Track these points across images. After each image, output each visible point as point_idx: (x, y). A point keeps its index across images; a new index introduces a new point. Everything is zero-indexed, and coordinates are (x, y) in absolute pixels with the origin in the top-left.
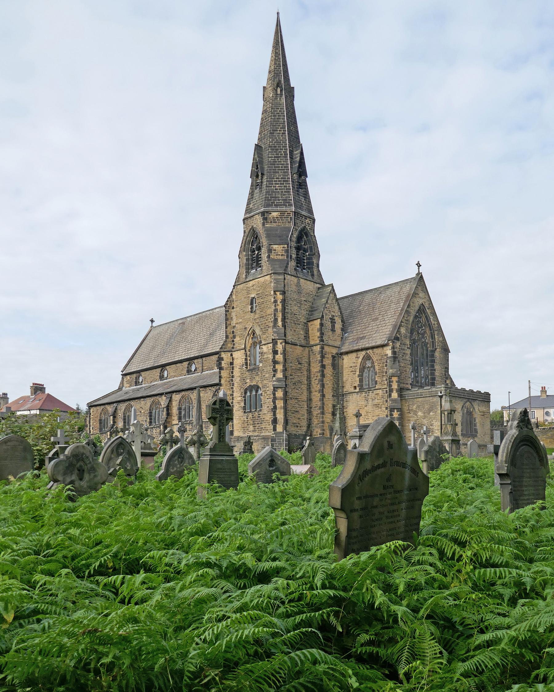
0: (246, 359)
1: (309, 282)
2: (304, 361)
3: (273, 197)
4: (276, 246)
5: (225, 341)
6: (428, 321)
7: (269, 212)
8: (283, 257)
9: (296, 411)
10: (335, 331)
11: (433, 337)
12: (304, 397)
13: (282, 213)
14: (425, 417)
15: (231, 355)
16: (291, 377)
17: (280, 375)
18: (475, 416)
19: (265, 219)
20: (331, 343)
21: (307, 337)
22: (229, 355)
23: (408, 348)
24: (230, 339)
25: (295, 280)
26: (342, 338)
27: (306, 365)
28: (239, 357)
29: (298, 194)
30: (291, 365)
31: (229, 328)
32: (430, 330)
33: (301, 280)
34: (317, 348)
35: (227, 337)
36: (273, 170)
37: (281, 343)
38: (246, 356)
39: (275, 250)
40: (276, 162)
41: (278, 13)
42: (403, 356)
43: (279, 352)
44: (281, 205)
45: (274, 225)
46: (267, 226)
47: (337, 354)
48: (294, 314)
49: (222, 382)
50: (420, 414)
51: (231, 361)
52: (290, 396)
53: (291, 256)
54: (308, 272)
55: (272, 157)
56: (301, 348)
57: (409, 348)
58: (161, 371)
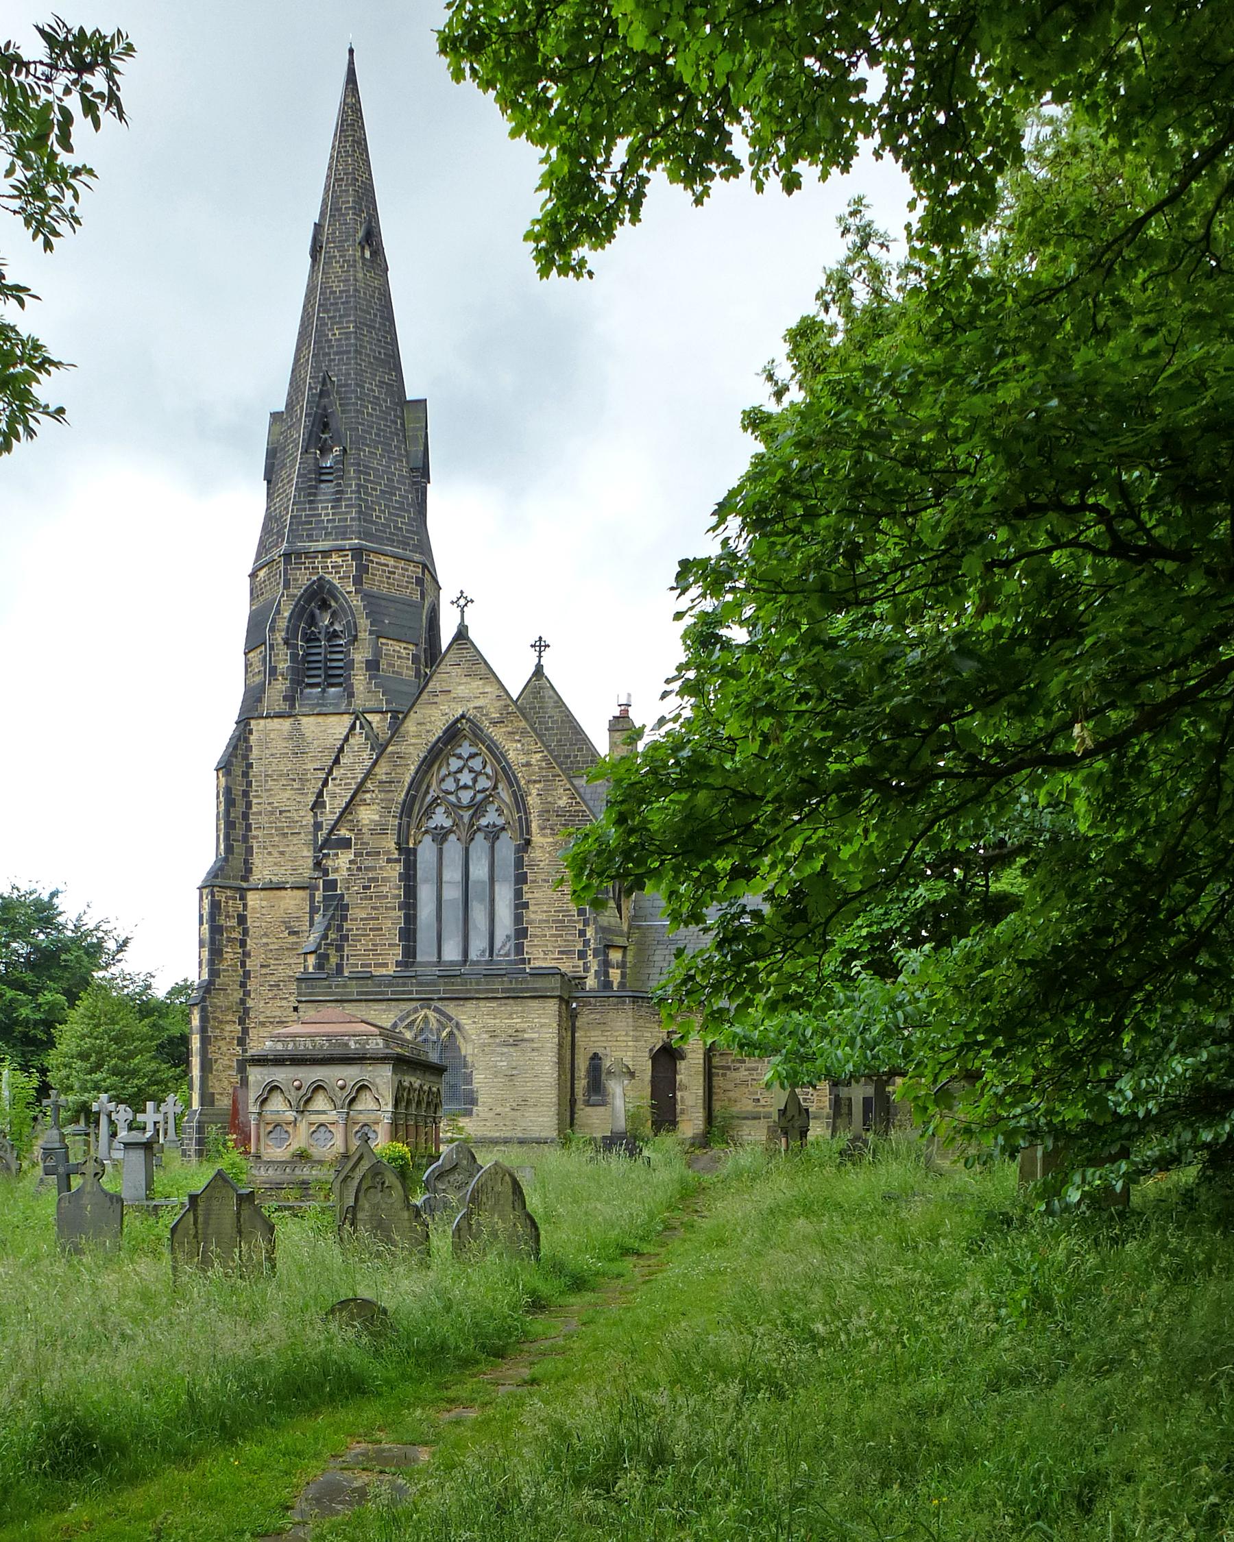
6: (499, 762)
16: (264, 971)
18: (466, 1049)
23: (389, 861)
25: (286, 724)
30: (265, 940)
32: (511, 786)
33: (304, 720)
48: (281, 812)
53: (273, 671)
57: (398, 861)
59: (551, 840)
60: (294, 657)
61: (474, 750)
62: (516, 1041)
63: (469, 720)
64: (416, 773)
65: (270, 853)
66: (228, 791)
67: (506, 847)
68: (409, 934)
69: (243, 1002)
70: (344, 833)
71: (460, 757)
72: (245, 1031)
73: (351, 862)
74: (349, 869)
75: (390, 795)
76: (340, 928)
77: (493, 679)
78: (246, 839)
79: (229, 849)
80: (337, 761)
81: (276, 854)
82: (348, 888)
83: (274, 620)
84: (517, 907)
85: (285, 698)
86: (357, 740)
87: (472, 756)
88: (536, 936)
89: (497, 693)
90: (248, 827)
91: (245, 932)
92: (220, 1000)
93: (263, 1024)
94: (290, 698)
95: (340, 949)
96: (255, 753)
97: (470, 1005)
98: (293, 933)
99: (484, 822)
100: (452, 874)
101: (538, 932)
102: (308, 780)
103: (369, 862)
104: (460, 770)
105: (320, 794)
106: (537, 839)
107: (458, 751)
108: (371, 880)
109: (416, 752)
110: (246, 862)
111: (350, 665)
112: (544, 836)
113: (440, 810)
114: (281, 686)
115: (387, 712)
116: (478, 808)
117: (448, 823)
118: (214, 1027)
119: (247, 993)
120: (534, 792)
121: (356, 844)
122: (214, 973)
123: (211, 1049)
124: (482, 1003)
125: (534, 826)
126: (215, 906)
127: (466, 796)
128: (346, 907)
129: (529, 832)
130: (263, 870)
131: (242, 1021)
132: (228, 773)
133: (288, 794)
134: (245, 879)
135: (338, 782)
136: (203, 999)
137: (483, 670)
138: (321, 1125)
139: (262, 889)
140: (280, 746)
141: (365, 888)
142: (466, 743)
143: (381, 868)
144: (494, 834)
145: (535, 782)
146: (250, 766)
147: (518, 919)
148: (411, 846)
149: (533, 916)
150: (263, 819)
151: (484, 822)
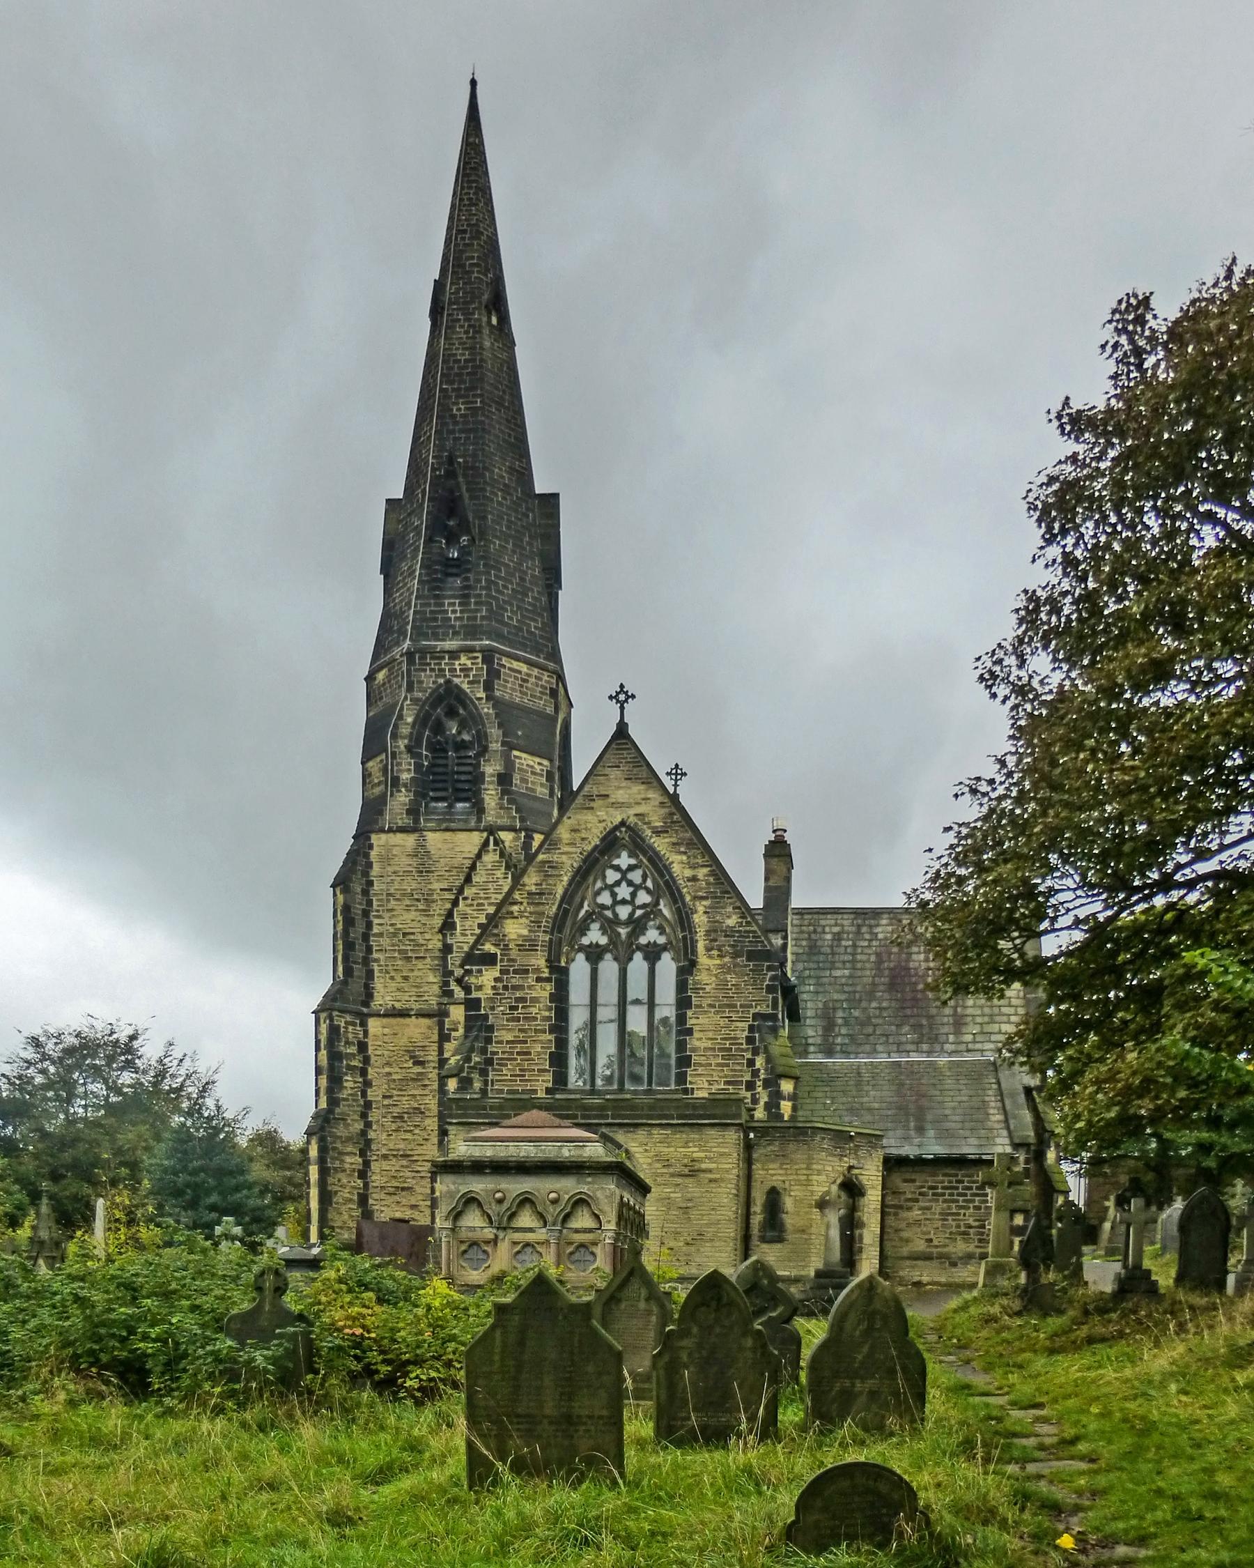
6: (662, 876)
9: (403, 1189)
16: (386, 1102)
23: (539, 980)
25: (410, 840)
30: (387, 1070)
32: (675, 902)
33: (430, 836)
48: (405, 934)
53: (396, 782)
57: (548, 980)
59: (718, 962)
60: (418, 767)
61: (633, 861)
62: (693, 1172)
63: (629, 828)
64: (570, 884)
65: (392, 978)
66: (347, 909)
67: (667, 966)
68: (559, 1060)
69: (363, 1133)
70: (489, 947)
71: (617, 868)
72: (367, 1164)
73: (496, 980)
74: (494, 988)
75: (541, 908)
76: (484, 1051)
77: (655, 784)
78: (366, 961)
79: (348, 972)
80: (468, 880)
81: (399, 979)
82: (493, 1008)
83: (396, 726)
84: (679, 1033)
85: (409, 812)
86: (490, 858)
87: (631, 868)
88: (700, 1065)
89: (661, 799)
90: (369, 950)
91: (366, 1060)
92: (340, 1131)
93: (385, 1157)
94: (413, 811)
95: (484, 1073)
96: (376, 870)
97: (641, 1134)
98: (417, 1063)
99: (643, 940)
100: (608, 994)
101: (702, 1060)
102: (433, 901)
103: (516, 980)
104: (618, 883)
105: (450, 914)
106: (703, 959)
107: (616, 862)
108: (518, 1000)
109: (570, 862)
110: (367, 986)
111: (479, 778)
112: (710, 957)
113: (595, 926)
114: (403, 798)
115: (520, 830)
116: (638, 926)
117: (603, 941)
118: (333, 1159)
119: (368, 1125)
120: (701, 909)
121: (502, 960)
122: (333, 1102)
123: (330, 1180)
124: (655, 1131)
125: (701, 946)
126: (334, 1031)
127: (624, 912)
128: (491, 1029)
129: (694, 952)
130: (385, 994)
131: (363, 1153)
132: (346, 891)
133: (413, 915)
134: (366, 1004)
135: (469, 902)
136: (322, 1129)
137: (644, 773)
138: (527, 1245)
139: (385, 1016)
140: (404, 863)
141: (512, 1008)
142: (624, 854)
143: (530, 987)
144: (653, 954)
145: (702, 898)
146: (370, 883)
147: (681, 1046)
148: (563, 964)
149: (697, 1044)
150: (385, 942)
151: (643, 940)
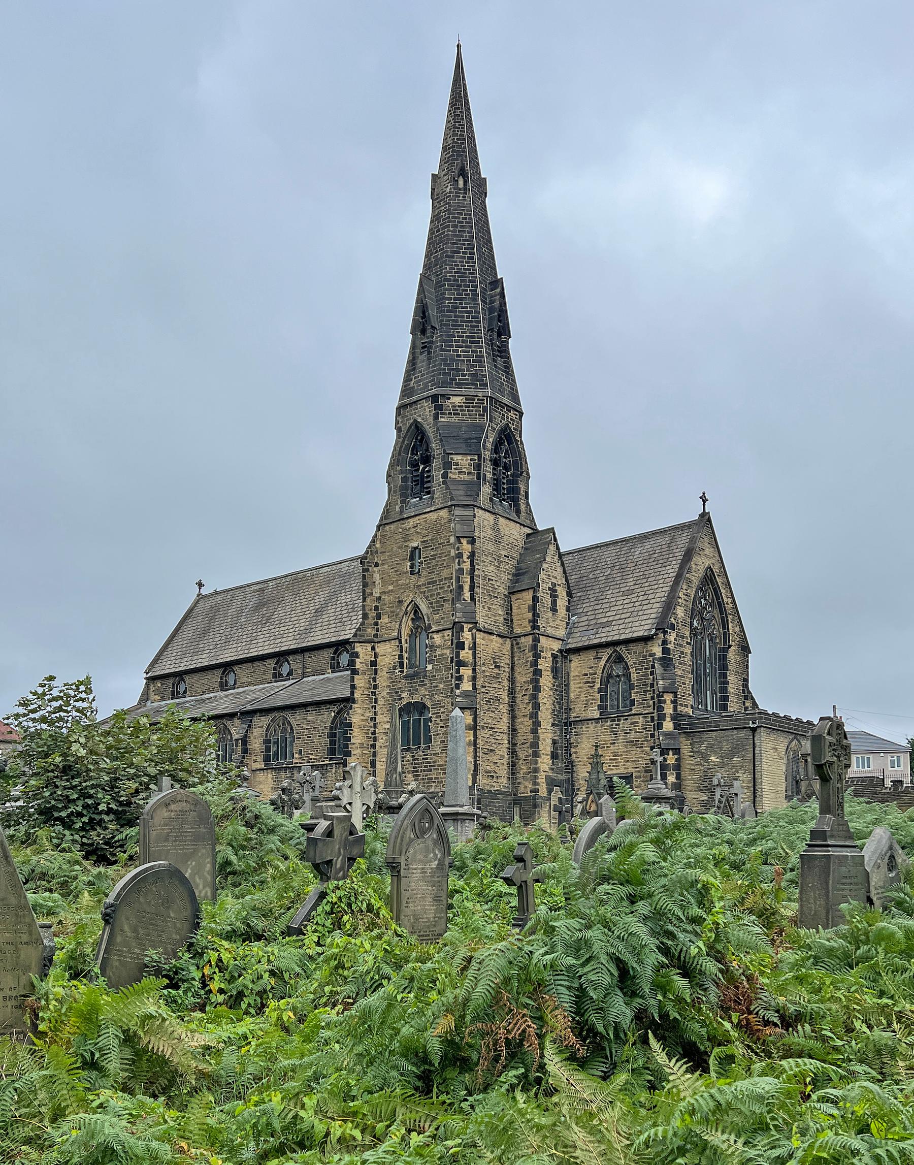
0: (401, 657)
1: (512, 524)
2: (505, 661)
3: (453, 370)
4: (459, 457)
5: (362, 624)
7: (446, 397)
8: (471, 477)
9: (491, 751)
10: (556, 611)
11: (725, 625)
12: (504, 725)
13: (470, 399)
14: (722, 765)
15: (373, 648)
16: (483, 690)
17: (467, 686)
19: (439, 408)
20: (550, 631)
21: (509, 621)
22: (369, 649)
24: (371, 621)
25: (491, 518)
26: (567, 624)
27: (507, 669)
28: (387, 653)
29: (496, 366)
30: (483, 668)
31: (368, 601)
32: (721, 613)
33: (501, 519)
34: (527, 641)
35: (365, 616)
36: (453, 321)
37: (470, 630)
38: (401, 651)
39: (457, 464)
40: (458, 307)
41: (459, 46)
42: (680, 657)
43: (466, 646)
44: (467, 384)
45: (455, 419)
46: (443, 420)
47: (560, 651)
48: (489, 579)
49: (356, 695)
50: (713, 758)
51: (373, 659)
52: (482, 724)
53: (485, 475)
54: (510, 505)
55: (450, 299)
56: (500, 640)
58: (223, 673)
